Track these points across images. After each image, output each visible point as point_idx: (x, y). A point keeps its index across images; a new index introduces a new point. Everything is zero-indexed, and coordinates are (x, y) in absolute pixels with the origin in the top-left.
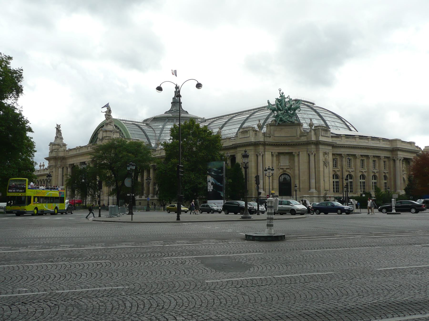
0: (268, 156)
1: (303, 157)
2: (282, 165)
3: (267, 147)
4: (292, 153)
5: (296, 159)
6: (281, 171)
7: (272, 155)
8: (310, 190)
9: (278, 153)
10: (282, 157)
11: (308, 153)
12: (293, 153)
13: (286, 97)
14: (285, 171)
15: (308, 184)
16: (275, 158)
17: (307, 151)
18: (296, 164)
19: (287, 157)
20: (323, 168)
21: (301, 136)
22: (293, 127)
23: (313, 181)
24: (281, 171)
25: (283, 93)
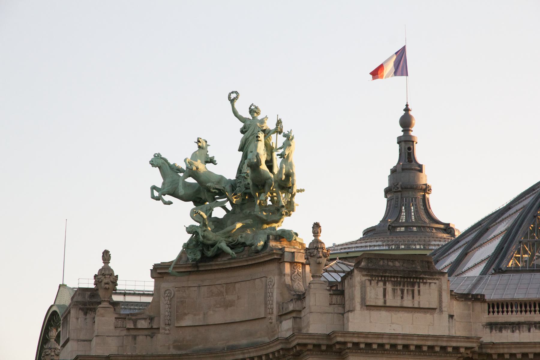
21: (281, 316)
22: (259, 271)
25: (253, 111)
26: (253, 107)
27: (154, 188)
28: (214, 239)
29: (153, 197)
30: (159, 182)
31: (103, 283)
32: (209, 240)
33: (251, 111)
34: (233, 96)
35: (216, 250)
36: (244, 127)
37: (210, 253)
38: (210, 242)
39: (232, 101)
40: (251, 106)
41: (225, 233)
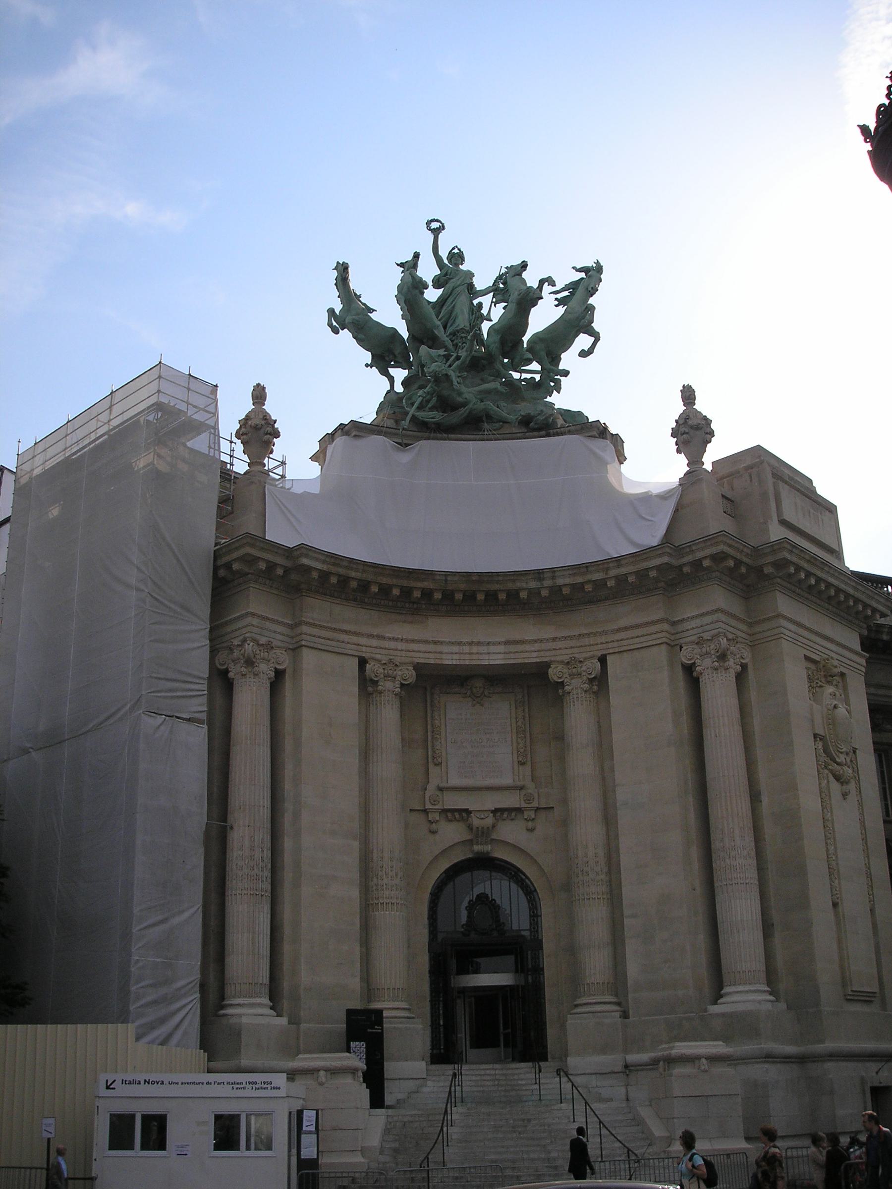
0: (324, 691)
1: (644, 702)
2: (454, 781)
3: (318, 610)
4: (544, 667)
5: (579, 716)
6: (451, 833)
7: (367, 686)
8: (717, 996)
9: (418, 667)
10: (455, 712)
11: (685, 656)
12: (554, 673)
13: (481, 283)
14: (483, 834)
15: (702, 940)
16: (388, 714)
17: (674, 646)
18: (582, 763)
19: (501, 712)
20: (824, 796)
23: (741, 909)
24: (451, 833)
25: (457, 257)
26: (456, 251)
27: (331, 312)
28: (466, 395)
29: (330, 325)
30: (338, 307)
31: (262, 431)
32: (460, 394)
33: (451, 256)
34: (435, 225)
35: (466, 414)
36: (446, 274)
37: (455, 418)
38: (460, 399)
39: (436, 232)
40: (453, 249)
41: (480, 392)
